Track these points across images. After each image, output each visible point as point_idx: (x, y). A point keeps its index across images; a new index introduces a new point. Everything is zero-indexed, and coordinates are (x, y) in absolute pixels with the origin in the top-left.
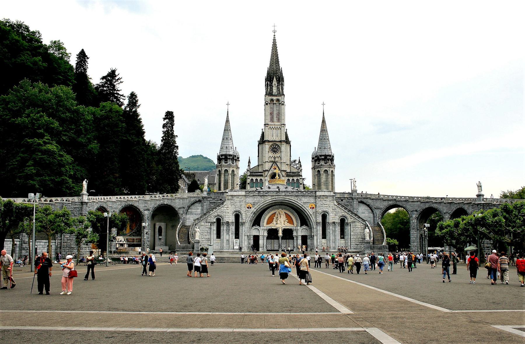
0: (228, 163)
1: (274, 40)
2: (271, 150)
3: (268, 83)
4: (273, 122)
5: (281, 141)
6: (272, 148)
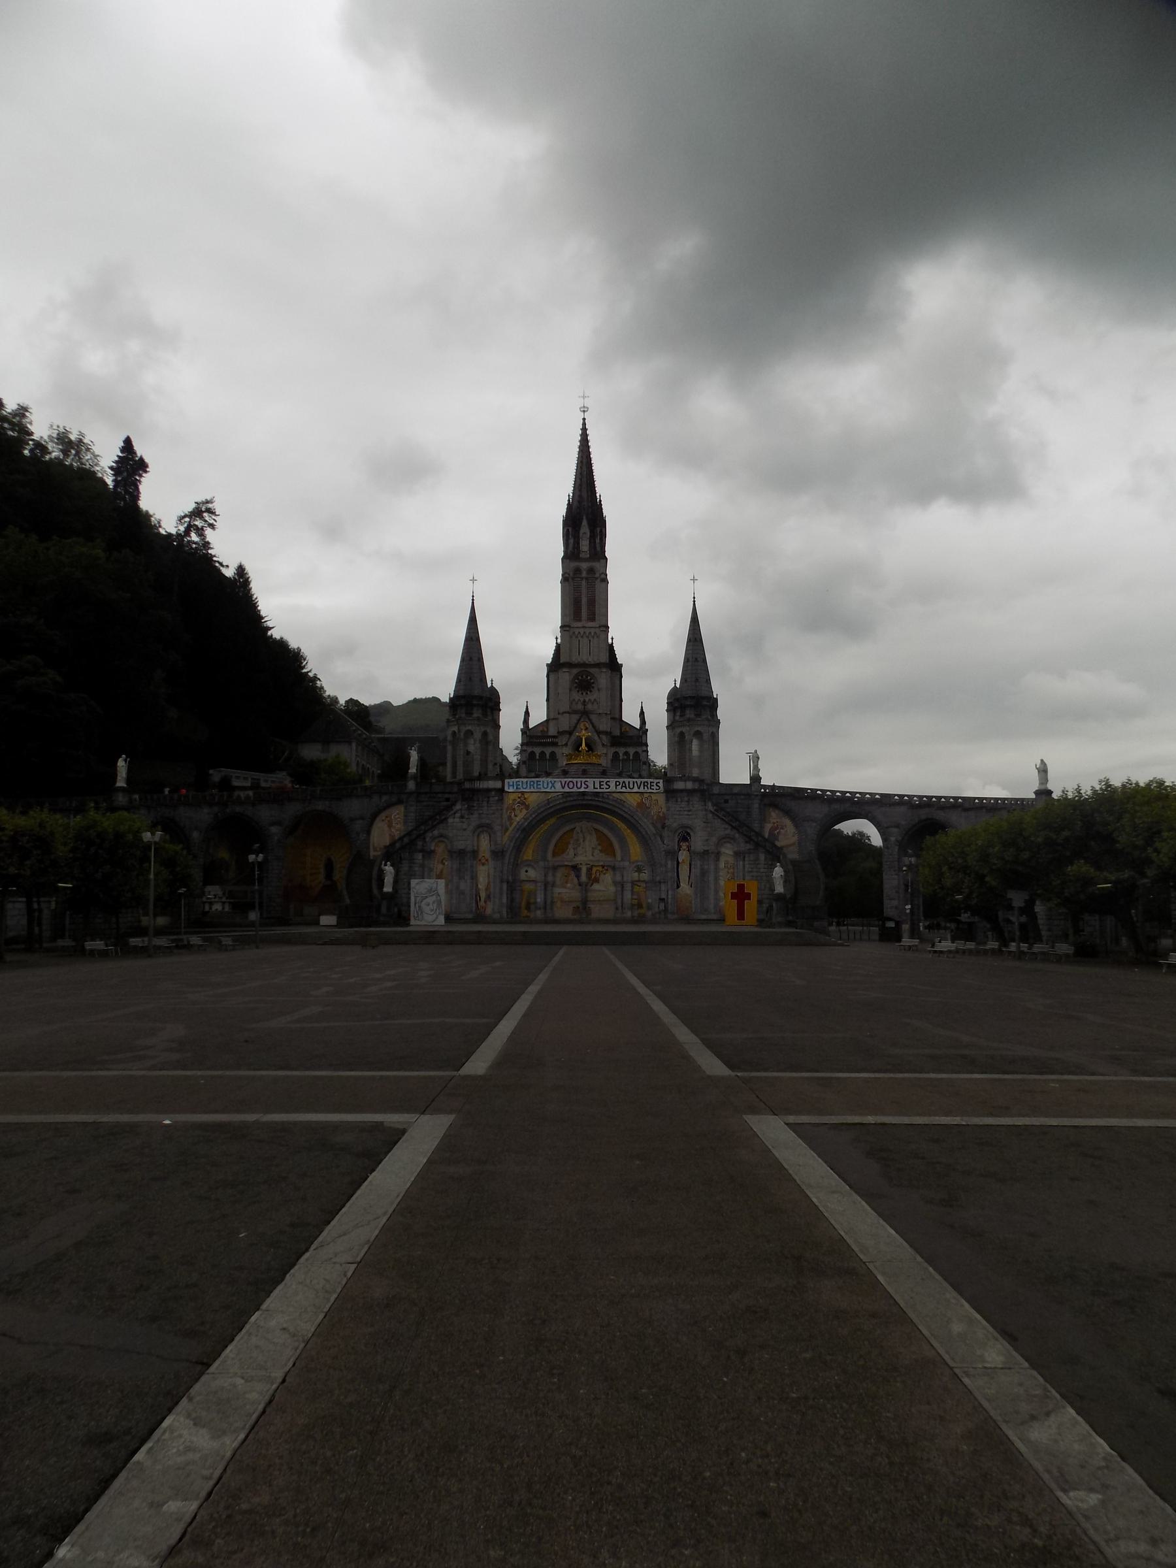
0: (475, 715)
1: (584, 429)
3: (568, 530)
4: (580, 620)
5: (598, 665)
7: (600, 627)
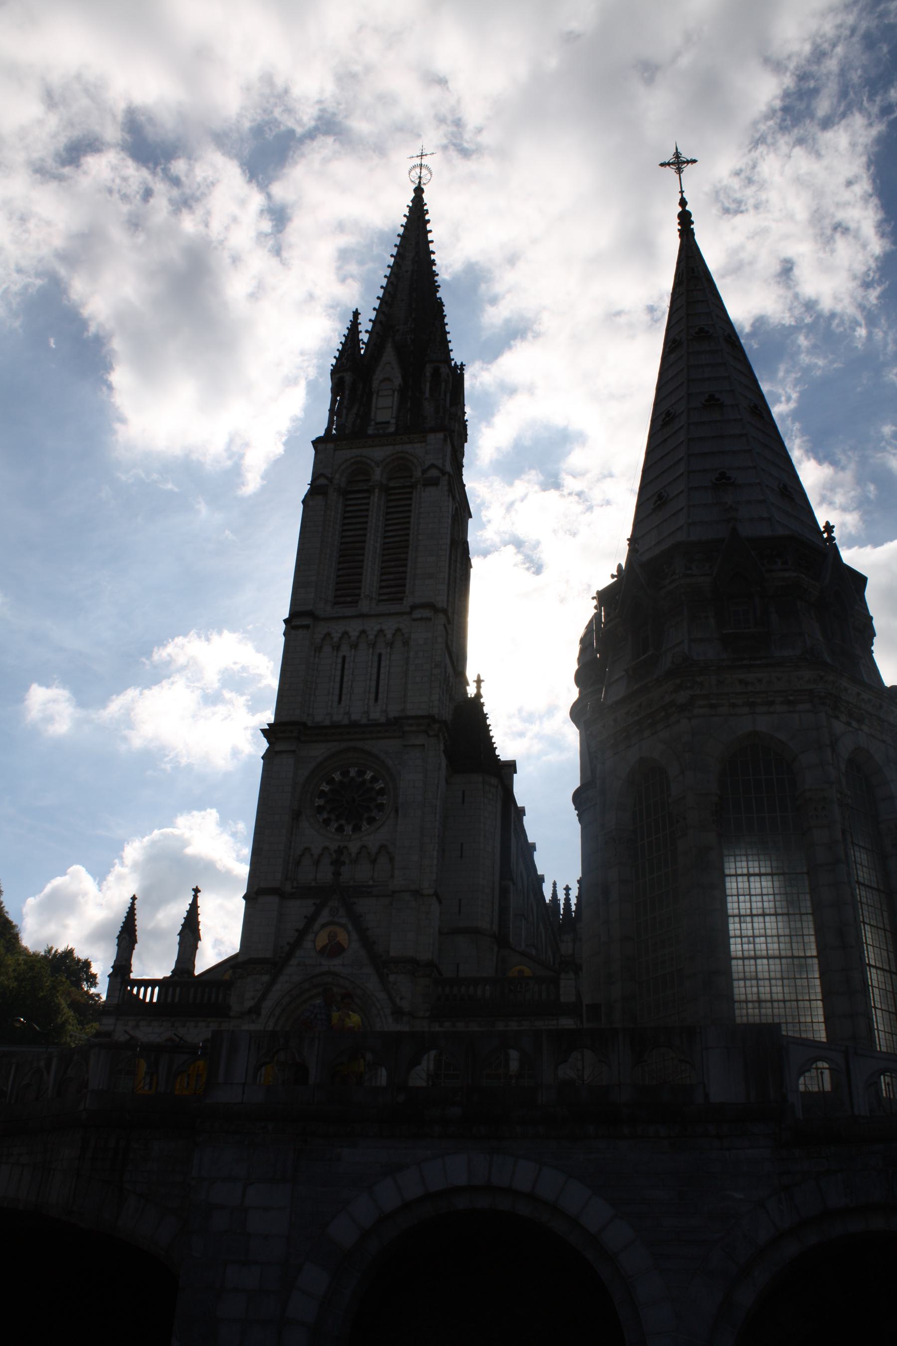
2: (321, 802)
6: (325, 788)
7: (414, 607)
